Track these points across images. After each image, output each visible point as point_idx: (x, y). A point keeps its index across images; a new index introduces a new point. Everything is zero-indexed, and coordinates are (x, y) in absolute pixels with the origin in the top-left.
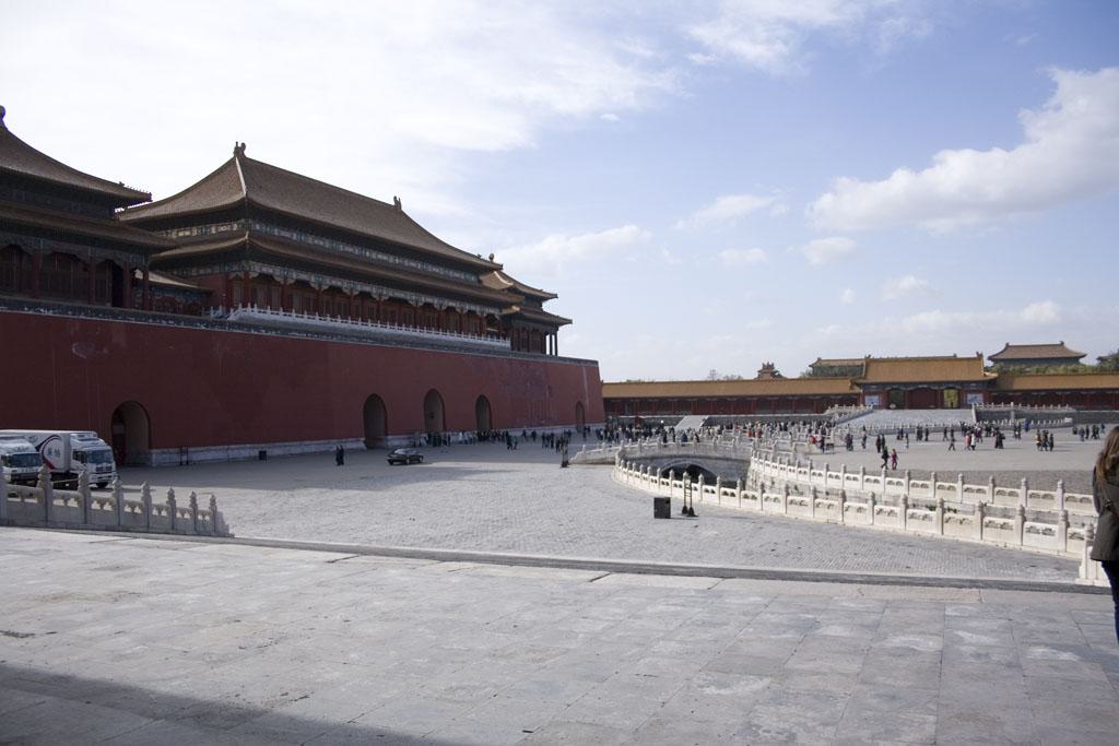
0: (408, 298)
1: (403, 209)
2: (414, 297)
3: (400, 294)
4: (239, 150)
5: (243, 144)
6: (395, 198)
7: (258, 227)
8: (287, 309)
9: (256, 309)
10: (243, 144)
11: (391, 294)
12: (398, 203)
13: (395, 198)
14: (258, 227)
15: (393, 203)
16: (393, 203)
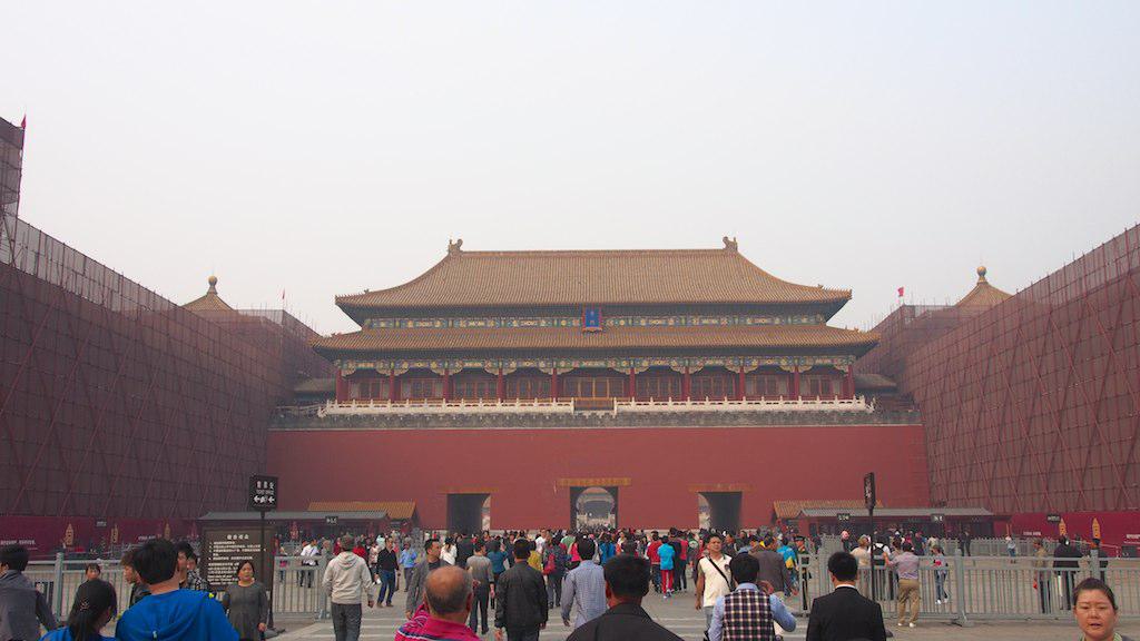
0: (611, 364)
1: (739, 251)
2: (624, 364)
3: (597, 364)
4: (455, 249)
5: (460, 242)
6: (726, 239)
7: (383, 325)
8: (396, 398)
9: (336, 405)
10: (460, 242)
11: (575, 364)
12: (731, 246)
13: (726, 239)
14: (383, 325)
15: (722, 246)
16: (724, 246)
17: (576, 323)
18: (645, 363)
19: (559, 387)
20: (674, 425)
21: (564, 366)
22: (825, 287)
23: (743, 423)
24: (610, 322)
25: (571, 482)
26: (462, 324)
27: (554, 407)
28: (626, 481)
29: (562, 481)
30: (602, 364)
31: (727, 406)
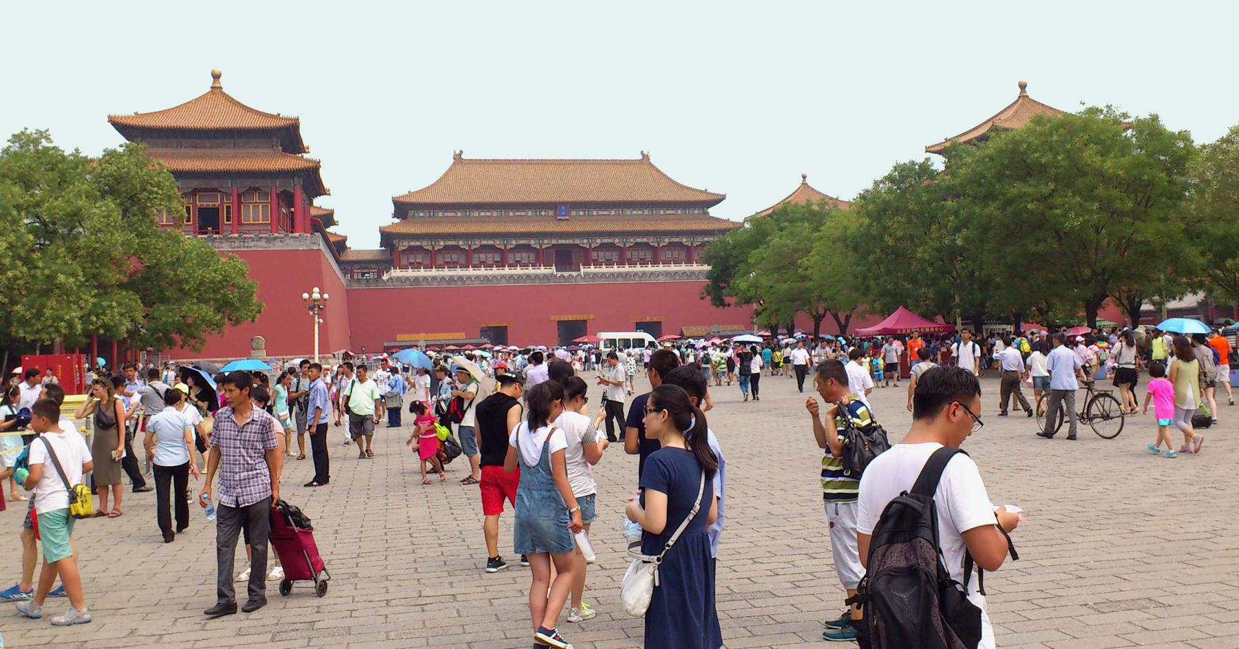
0: (577, 242)
11: (554, 242)
12: (645, 157)
17: (551, 213)
18: (599, 241)
19: (541, 258)
20: (620, 281)
21: (547, 243)
22: (710, 190)
23: (662, 279)
24: (573, 213)
25: (558, 318)
26: (476, 214)
27: (543, 270)
28: (592, 316)
29: (552, 318)
30: (571, 242)
31: (650, 268)
